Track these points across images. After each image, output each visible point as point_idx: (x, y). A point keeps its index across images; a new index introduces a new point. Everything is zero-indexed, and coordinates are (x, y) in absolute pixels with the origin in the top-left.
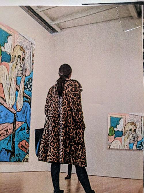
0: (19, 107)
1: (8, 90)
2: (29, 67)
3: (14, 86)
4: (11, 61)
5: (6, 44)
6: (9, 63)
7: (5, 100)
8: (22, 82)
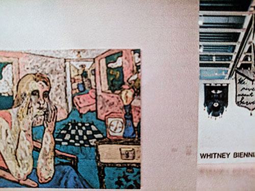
0: (43, 175)
1: (13, 153)
2: (64, 104)
3: (26, 145)
4: (15, 105)
6: (10, 110)
7: (8, 170)
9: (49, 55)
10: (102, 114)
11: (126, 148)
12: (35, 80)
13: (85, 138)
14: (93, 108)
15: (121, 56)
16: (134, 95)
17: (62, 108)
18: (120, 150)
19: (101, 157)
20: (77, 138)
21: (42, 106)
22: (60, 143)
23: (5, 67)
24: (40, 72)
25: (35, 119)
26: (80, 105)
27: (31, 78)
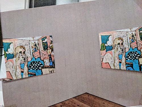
2: (30, 56)
4: (15, 56)
5: (9, 50)
8: (26, 66)
9: (24, 39)
10: (42, 58)
11: (51, 69)
12: (20, 48)
13: (38, 67)
14: (39, 56)
15: (46, 38)
16: (51, 51)
17: (30, 57)
18: (49, 70)
19: (43, 73)
20: (35, 67)
21: (23, 57)
22: (30, 69)
23: (10, 44)
24: (22, 45)
25: (21, 61)
26: (35, 56)
27: (19, 47)
